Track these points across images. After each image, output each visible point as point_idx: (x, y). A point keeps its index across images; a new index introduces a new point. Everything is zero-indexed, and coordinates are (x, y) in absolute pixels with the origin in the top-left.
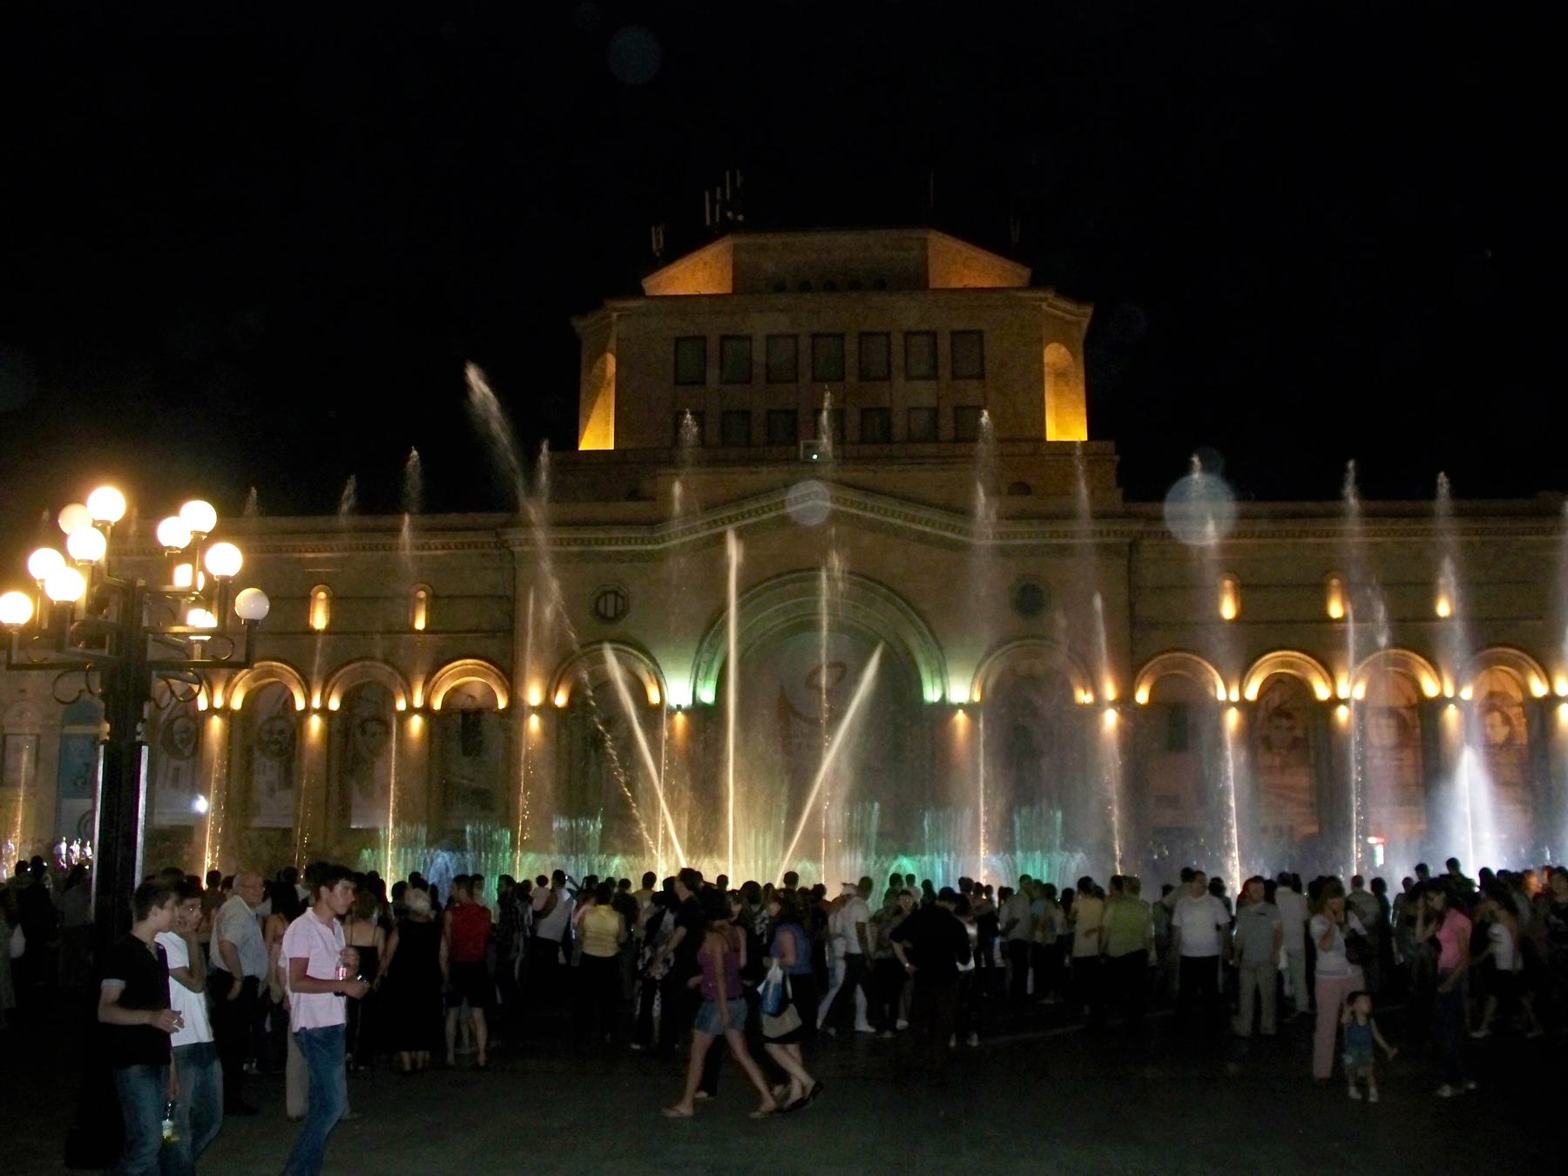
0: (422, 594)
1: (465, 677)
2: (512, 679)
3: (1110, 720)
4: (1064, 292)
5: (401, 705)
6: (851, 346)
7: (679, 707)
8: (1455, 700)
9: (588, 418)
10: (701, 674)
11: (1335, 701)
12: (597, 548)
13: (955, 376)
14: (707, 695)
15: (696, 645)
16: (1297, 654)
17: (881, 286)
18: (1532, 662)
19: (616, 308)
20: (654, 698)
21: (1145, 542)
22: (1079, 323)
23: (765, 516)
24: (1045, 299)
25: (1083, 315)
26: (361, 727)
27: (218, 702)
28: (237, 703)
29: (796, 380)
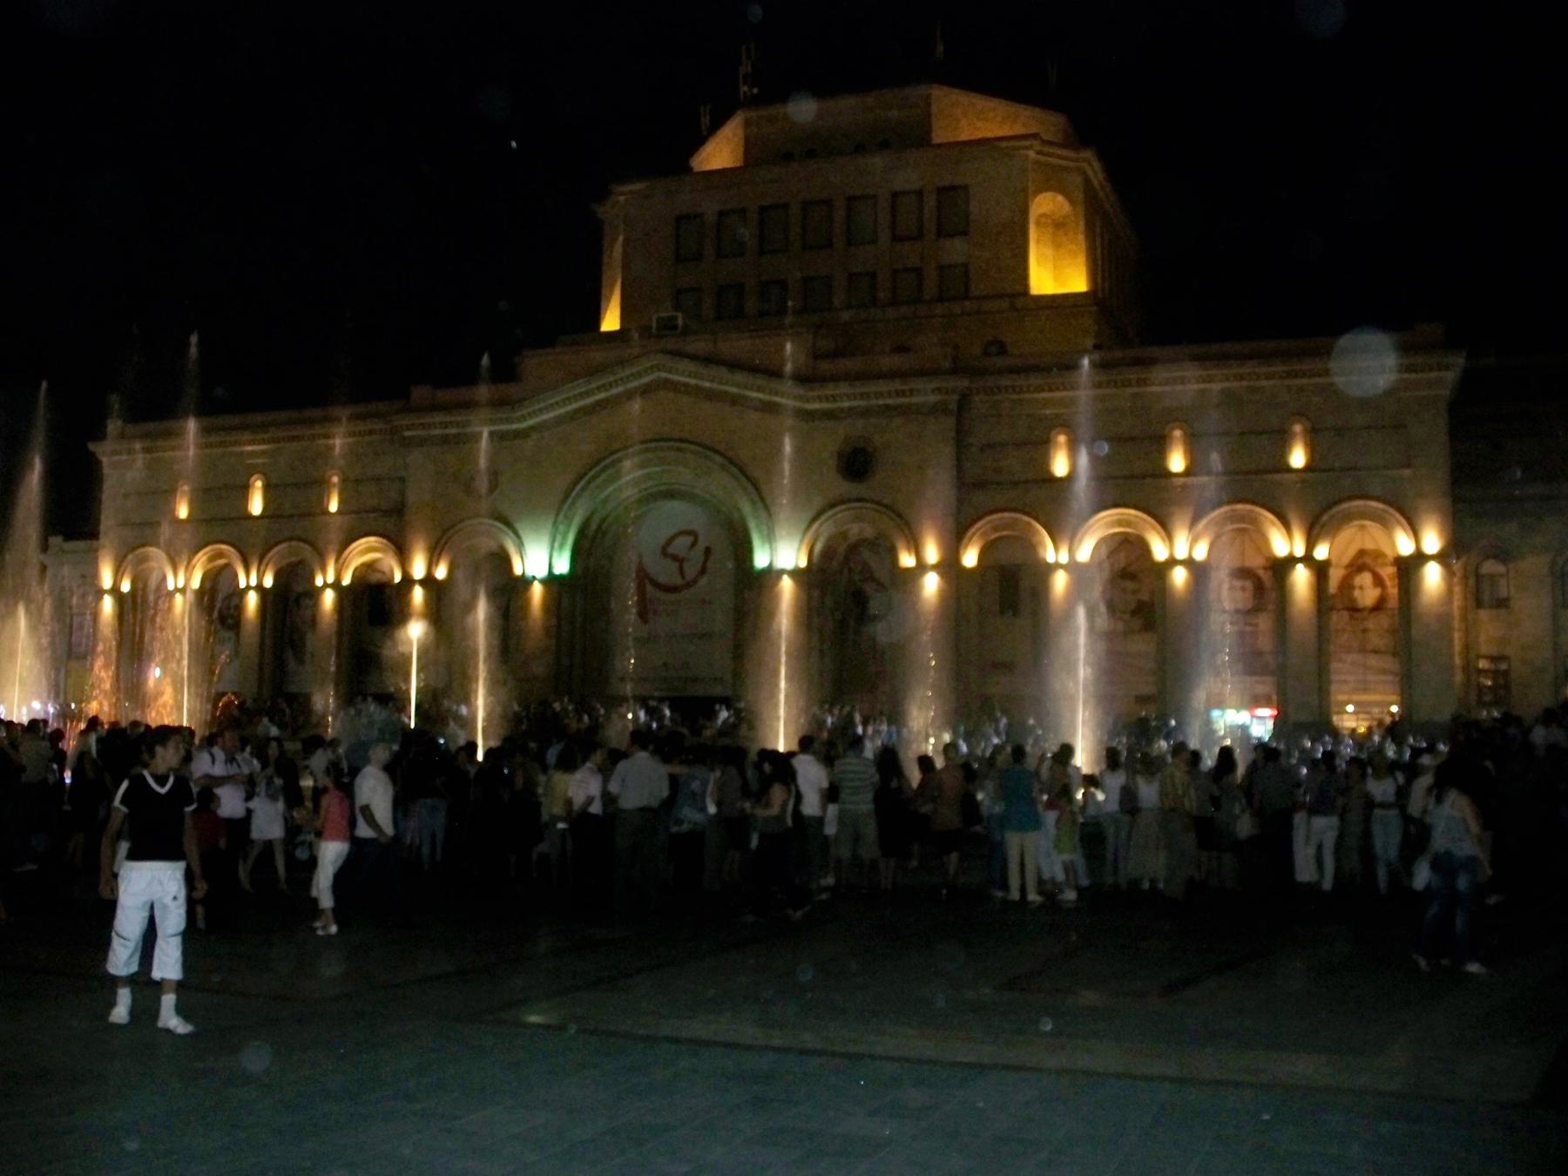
0: (335, 479)
1: (366, 552)
2: (403, 556)
3: (931, 585)
5: (319, 581)
6: (840, 215)
8: (1308, 559)
11: (1172, 562)
14: (562, 566)
15: (811, 515)
16: (1133, 512)
18: (1398, 516)
20: (518, 571)
23: (615, 391)
24: (1031, 147)
26: (290, 599)
27: (180, 585)
28: (196, 583)
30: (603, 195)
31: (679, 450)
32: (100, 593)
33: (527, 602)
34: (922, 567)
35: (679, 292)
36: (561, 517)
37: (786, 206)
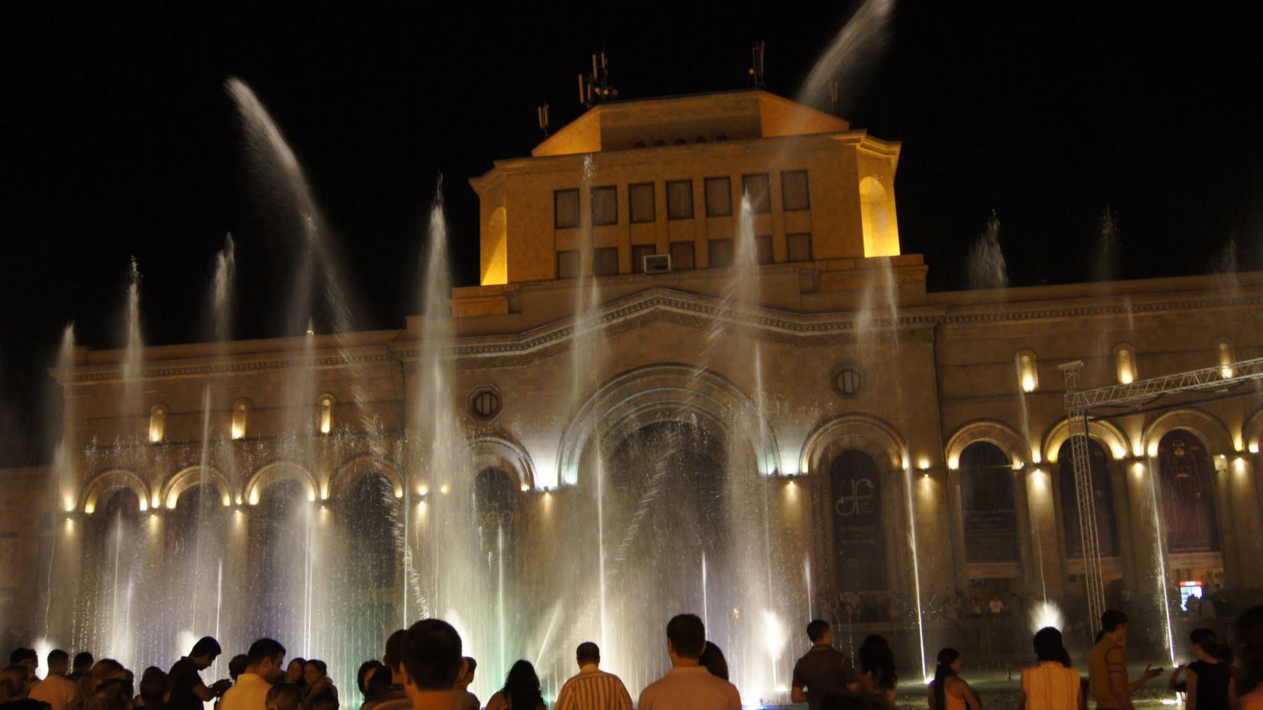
0: (327, 403)
3: (927, 484)
6: (698, 190)
7: (546, 489)
9: (488, 261)
10: (565, 460)
11: (1131, 459)
12: (473, 356)
14: (571, 478)
17: (722, 138)
19: (507, 169)
21: (949, 326)
22: (888, 161)
24: (858, 141)
29: (654, 220)
30: (483, 168)
32: (64, 516)
33: (539, 510)
34: (918, 473)
36: (568, 434)
37: (652, 184)
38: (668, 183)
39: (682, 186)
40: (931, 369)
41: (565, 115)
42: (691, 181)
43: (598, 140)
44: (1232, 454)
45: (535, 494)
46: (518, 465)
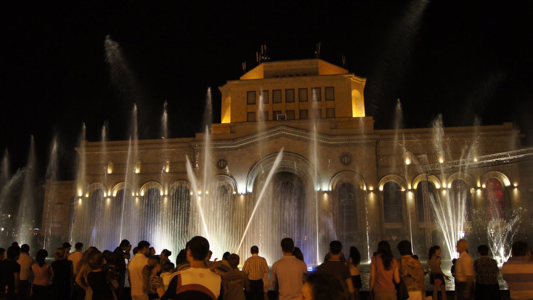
0: (168, 162)
3: (372, 196)
4: (357, 75)
6: (297, 93)
9: (224, 115)
10: (248, 184)
13: (326, 100)
14: (250, 190)
17: (305, 75)
19: (231, 84)
21: (381, 142)
22: (362, 84)
24: (352, 77)
25: (363, 82)
27: (109, 194)
28: (115, 195)
30: (223, 83)
31: (288, 155)
33: (239, 200)
34: (369, 191)
35: (248, 113)
36: (249, 175)
38: (286, 90)
39: (291, 91)
40: (374, 156)
41: (252, 66)
42: (294, 89)
43: (263, 74)
44: (476, 188)
45: (238, 195)
46: (232, 185)
